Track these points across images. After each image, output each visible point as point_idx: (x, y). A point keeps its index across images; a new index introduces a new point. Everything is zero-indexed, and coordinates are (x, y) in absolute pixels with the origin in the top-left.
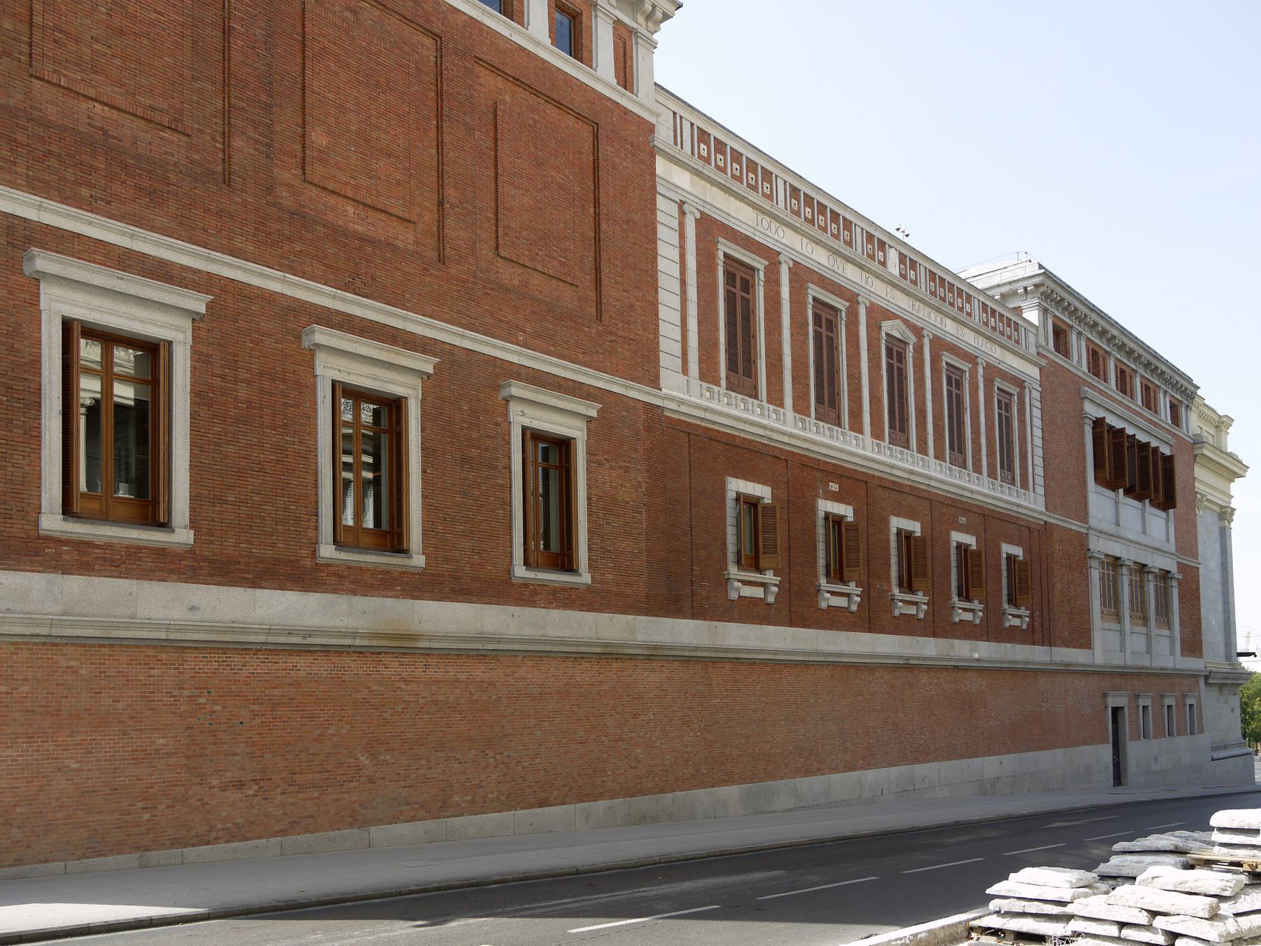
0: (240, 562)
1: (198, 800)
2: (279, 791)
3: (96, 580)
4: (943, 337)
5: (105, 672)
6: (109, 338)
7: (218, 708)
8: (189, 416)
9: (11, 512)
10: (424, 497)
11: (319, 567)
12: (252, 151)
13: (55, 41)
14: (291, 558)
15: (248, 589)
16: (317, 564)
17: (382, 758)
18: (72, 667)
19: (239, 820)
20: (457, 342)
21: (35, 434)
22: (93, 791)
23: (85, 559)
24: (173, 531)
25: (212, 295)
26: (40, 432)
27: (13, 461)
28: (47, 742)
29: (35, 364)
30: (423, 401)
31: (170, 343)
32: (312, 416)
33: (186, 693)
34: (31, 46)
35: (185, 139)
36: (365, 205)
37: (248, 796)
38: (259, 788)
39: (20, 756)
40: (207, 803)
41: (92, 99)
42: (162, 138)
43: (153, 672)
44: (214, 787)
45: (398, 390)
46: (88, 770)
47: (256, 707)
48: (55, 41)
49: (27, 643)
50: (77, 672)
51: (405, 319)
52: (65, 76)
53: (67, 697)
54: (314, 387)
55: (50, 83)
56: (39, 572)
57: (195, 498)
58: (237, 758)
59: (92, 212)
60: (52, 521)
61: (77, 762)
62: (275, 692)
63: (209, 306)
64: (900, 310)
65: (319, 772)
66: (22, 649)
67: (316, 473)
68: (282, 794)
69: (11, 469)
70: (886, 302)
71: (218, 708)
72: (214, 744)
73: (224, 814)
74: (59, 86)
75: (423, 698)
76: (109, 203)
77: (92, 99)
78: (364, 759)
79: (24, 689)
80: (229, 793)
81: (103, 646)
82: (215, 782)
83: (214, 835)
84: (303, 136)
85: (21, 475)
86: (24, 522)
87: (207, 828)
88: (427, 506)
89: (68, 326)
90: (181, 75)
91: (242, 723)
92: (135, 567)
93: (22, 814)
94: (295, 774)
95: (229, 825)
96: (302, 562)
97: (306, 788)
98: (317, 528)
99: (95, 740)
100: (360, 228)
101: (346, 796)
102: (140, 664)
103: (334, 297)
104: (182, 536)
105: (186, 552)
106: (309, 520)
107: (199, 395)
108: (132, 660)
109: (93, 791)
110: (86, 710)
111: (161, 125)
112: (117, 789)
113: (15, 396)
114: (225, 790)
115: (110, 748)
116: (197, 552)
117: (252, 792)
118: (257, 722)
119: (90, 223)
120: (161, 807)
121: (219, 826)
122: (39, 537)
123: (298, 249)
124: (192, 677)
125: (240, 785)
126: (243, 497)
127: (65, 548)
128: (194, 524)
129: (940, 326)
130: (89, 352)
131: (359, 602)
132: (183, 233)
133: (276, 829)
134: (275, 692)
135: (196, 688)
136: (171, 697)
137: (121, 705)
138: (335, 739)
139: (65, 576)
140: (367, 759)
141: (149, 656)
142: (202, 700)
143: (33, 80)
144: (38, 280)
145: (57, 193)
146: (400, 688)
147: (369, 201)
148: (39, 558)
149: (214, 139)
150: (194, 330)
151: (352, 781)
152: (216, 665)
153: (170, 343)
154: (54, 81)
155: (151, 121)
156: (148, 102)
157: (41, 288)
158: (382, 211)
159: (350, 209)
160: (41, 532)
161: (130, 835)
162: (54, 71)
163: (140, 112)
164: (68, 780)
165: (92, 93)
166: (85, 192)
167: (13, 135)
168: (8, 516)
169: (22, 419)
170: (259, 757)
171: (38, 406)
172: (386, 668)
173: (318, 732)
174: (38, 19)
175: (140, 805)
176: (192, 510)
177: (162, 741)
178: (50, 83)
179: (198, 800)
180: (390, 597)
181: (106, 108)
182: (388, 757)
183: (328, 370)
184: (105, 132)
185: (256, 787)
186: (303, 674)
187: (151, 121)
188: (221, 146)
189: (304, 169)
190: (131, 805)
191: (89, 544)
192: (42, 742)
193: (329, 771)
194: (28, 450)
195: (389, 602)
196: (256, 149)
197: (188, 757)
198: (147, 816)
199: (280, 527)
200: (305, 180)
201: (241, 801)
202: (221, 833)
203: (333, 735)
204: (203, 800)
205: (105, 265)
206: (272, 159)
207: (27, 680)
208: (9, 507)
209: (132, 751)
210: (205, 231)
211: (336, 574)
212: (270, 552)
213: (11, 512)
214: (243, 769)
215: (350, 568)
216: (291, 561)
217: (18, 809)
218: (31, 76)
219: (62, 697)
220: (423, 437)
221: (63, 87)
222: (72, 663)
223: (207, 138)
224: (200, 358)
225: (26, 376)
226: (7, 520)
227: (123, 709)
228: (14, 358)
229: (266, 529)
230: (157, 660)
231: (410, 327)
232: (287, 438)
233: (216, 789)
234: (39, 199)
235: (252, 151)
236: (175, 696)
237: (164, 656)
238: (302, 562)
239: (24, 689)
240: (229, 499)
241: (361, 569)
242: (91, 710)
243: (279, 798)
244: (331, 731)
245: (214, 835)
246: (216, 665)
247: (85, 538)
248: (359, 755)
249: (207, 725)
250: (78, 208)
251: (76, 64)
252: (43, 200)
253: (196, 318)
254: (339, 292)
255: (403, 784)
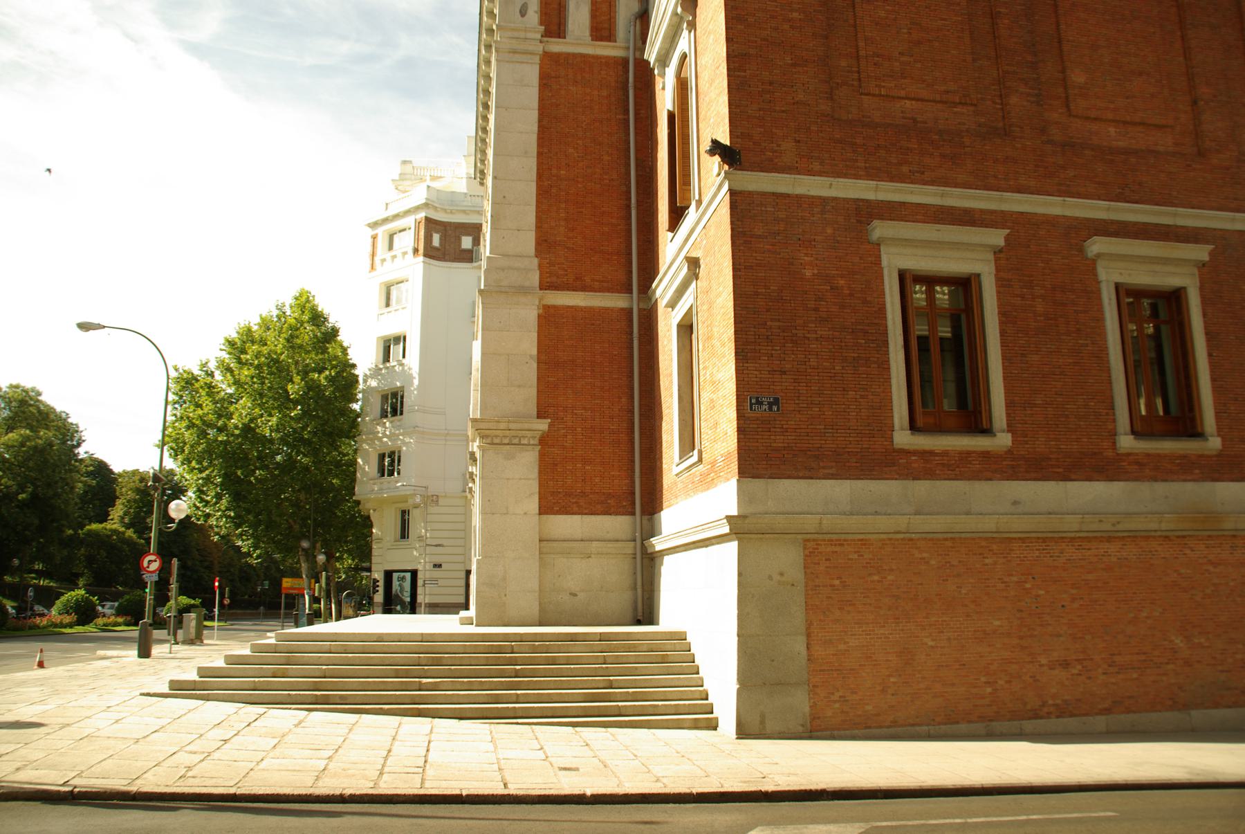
0: (1051, 458)
1: (1031, 677)
2: (1100, 670)
3: (938, 483)
5: (949, 562)
6: (930, 281)
7: (1042, 592)
8: (998, 335)
9: (873, 432)
10: (1213, 380)
11: (1120, 457)
12: (1025, 103)
13: (875, 64)
14: (1095, 450)
15: (1061, 483)
16: (1118, 454)
17: (1196, 641)
18: (924, 558)
19: (1066, 697)
20: (1228, 226)
21: (886, 366)
22: (947, 666)
23: (928, 466)
24: (995, 435)
25: (1009, 229)
26: (889, 365)
27: (873, 390)
28: (910, 622)
29: (882, 310)
30: (1202, 288)
31: (978, 275)
32: (1100, 319)
33: (1015, 579)
34: (859, 72)
35: (972, 108)
36: (1125, 123)
37: (1072, 675)
38: (1083, 667)
39: (891, 634)
40: (1038, 680)
41: (903, 98)
42: (955, 113)
43: (987, 561)
44: (1041, 666)
45: (1173, 281)
46: (941, 647)
47: (1074, 591)
48: (875, 64)
49: (890, 539)
50: (928, 562)
51: (1175, 215)
52: (884, 87)
53: (921, 584)
54: (1099, 292)
55: (874, 95)
56: (896, 479)
57: (1009, 405)
58: (1062, 639)
59: (912, 183)
60: (903, 438)
61: (933, 640)
62: (1090, 577)
63: (1007, 239)
65: (1138, 654)
66: (886, 544)
67: (1109, 370)
68: (1104, 674)
69: (871, 397)
71: (1042, 592)
72: (1042, 625)
73: (1054, 691)
74: (880, 95)
75: (1233, 580)
76: (923, 173)
77: (903, 98)
78: (1178, 641)
79: (890, 577)
80: (1056, 672)
81: (946, 539)
82: (1044, 661)
83: (1046, 710)
84: (1064, 80)
85: (878, 401)
86: (883, 439)
87: (1041, 704)
88: (1217, 389)
89: (902, 275)
90: (964, 61)
91: (1063, 606)
92: (967, 469)
93: (894, 683)
94: (1114, 655)
95: (1059, 702)
96: (1105, 454)
97: (1126, 669)
98: (1114, 421)
99: (945, 621)
100: (1121, 144)
101: (1164, 678)
102: (976, 554)
103: (1108, 209)
104: (1002, 440)
105: (1006, 453)
106: (1107, 414)
107: (1005, 316)
108: (969, 551)
109: (947, 666)
110: (937, 595)
111: (954, 103)
112: (964, 665)
113: (870, 338)
114: (1054, 669)
115: (958, 628)
116: (1015, 453)
117: (1075, 671)
118: (1076, 605)
119: (912, 192)
120: (1001, 682)
121: (1050, 702)
122: (895, 451)
123: (1072, 174)
124: (1018, 564)
125: (1065, 664)
126: (1048, 399)
127: (913, 458)
128: (1011, 428)
130: (919, 294)
131: (1161, 488)
132: (979, 183)
133: (1100, 707)
134: (1090, 577)
135: (1022, 575)
136: (1002, 583)
137: (964, 591)
138: (1149, 622)
139: (915, 482)
140: (1182, 641)
141: (982, 547)
142: (1028, 586)
143: (863, 97)
144: (879, 245)
145: (886, 175)
146: (1207, 570)
147: (1128, 119)
148: (895, 468)
149: (994, 103)
150: (996, 261)
151: (1167, 663)
152: (1037, 553)
153: (978, 275)
154: (877, 93)
155: (946, 102)
156: (943, 88)
157: (882, 250)
158: (1140, 124)
159: (1112, 130)
160: (895, 446)
161: (976, 706)
162: (876, 86)
163: (938, 98)
164: (927, 655)
165: (903, 94)
166: (905, 169)
167: (854, 140)
168: (872, 435)
169: (877, 356)
170: (1080, 638)
171: (886, 343)
172: (1193, 551)
173: (1132, 615)
174: (862, 53)
175: (983, 679)
176: (1008, 415)
177: (997, 623)
178: (874, 95)
179: (1031, 677)
180: (1190, 481)
181: (913, 102)
182: (1203, 640)
183: (1109, 276)
184: (914, 120)
185: (1079, 667)
186: (1114, 559)
187: (946, 102)
188: (999, 106)
189: (1068, 107)
190: (977, 679)
191: (931, 453)
192: (906, 622)
193: (1144, 653)
194: (882, 380)
195: (1189, 486)
196: (1028, 101)
197: (1021, 638)
198: (989, 690)
199: (1082, 423)
200: (1070, 115)
201: (1067, 679)
202: (1052, 709)
203: (1147, 617)
204: (1035, 677)
205: (925, 222)
206: (1042, 105)
207: (892, 570)
208: (872, 428)
209: (975, 631)
210: (995, 177)
211: (1137, 463)
212: (1076, 447)
213: (873, 432)
214: (1068, 649)
215: (1148, 455)
216: (1095, 454)
217: (892, 680)
218: (861, 94)
219: (919, 584)
220: (1205, 322)
221: (883, 96)
222: (925, 555)
223: (989, 103)
224: (1002, 284)
225: (876, 321)
226: (871, 439)
227: (965, 594)
228: (867, 309)
229: (1071, 426)
230: (990, 550)
231: (1181, 222)
232: (1080, 342)
233: (1045, 668)
234: (875, 182)
235: (1025, 103)
236: (1005, 582)
237: (995, 547)
238: (1105, 454)
239: (890, 577)
240: (1037, 402)
241: (1159, 455)
242: (940, 595)
243: (1102, 677)
244: (1144, 614)
245: (1046, 710)
246: (1037, 553)
247: (927, 448)
248: (1173, 638)
249: (1034, 608)
250: (901, 182)
251: (891, 76)
252: (879, 183)
253: (998, 252)
254: (1112, 203)
255: (1220, 668)
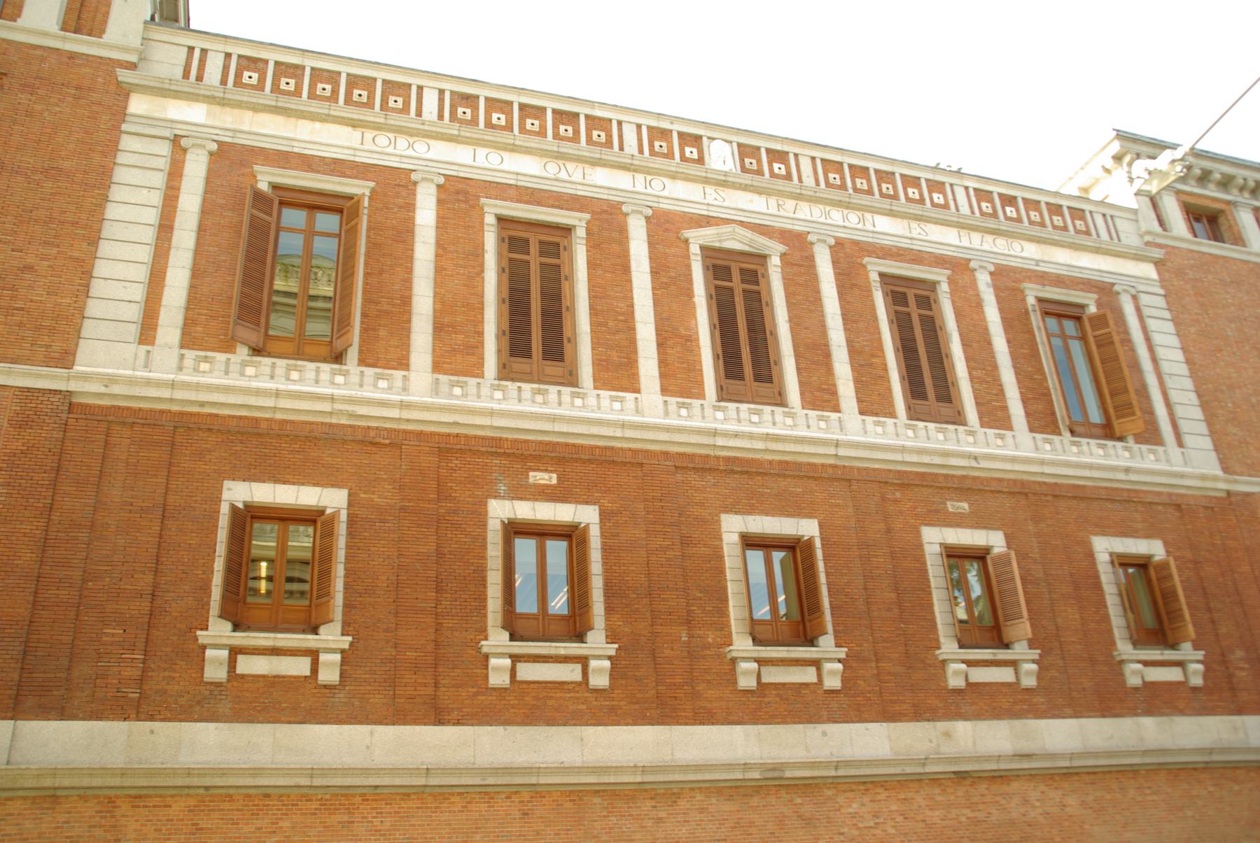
4: (871, 240)
64: (741, 213)
70: (705, 207)
129: (860, 226)
